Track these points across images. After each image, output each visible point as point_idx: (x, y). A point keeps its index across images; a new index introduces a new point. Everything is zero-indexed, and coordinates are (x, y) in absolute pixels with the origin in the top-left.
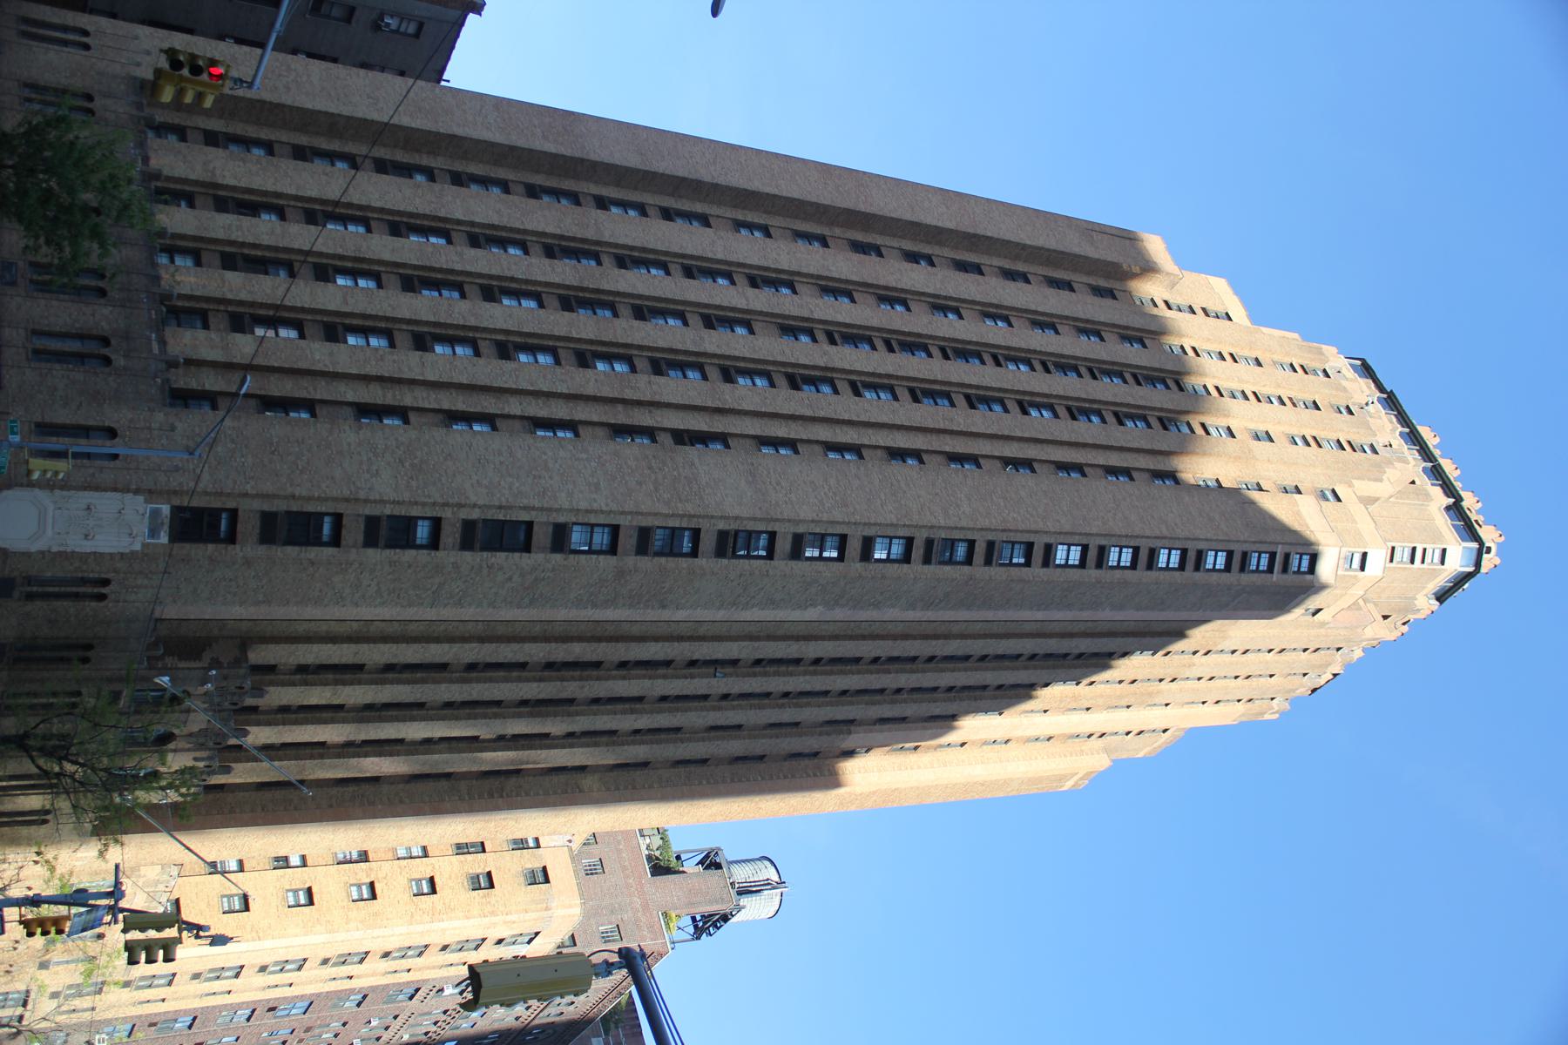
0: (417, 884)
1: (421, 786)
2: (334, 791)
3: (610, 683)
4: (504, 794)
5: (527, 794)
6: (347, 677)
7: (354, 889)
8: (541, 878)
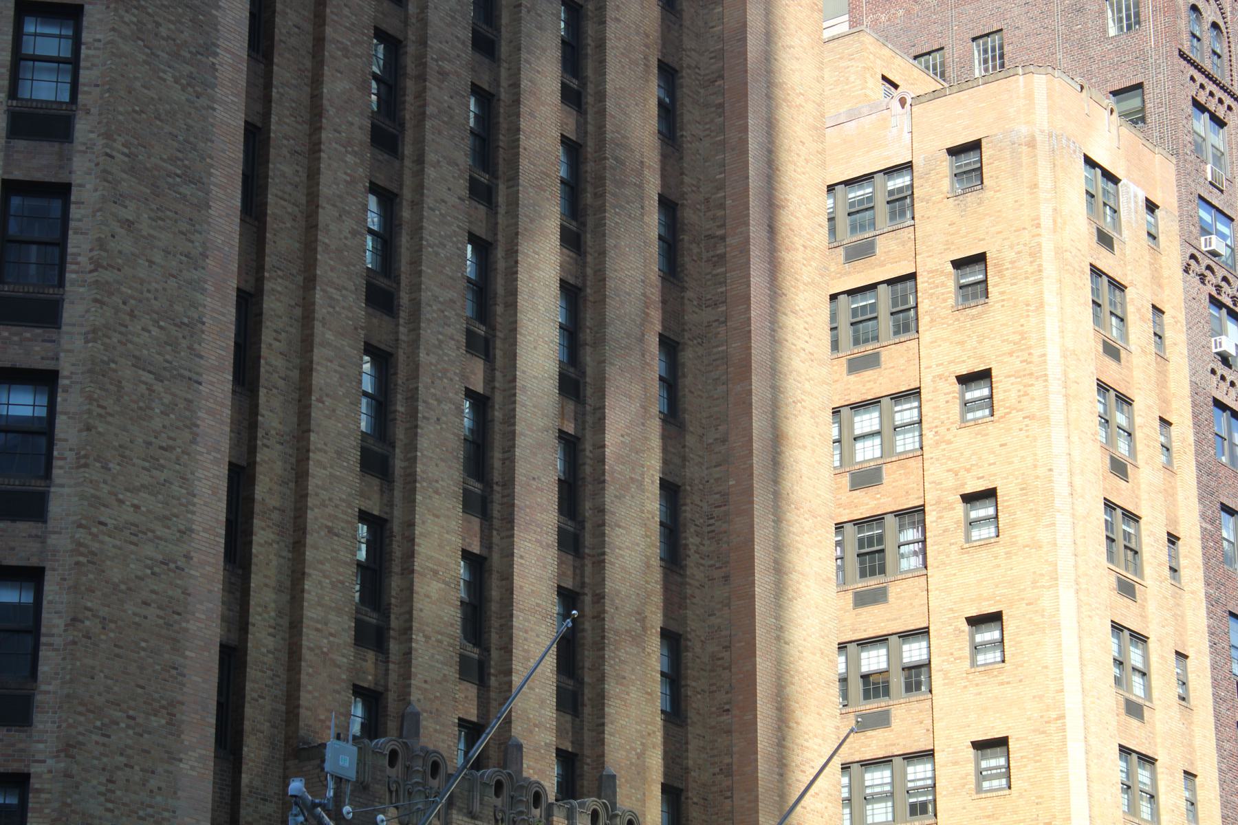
0: (970, 410)
1: (691, 401)
2: (695, 570)
3: (434, 17)
4: (720, 232)
5: (721, 187)
6: (397, 550)
7: (976, 534)
8: (969, 159)
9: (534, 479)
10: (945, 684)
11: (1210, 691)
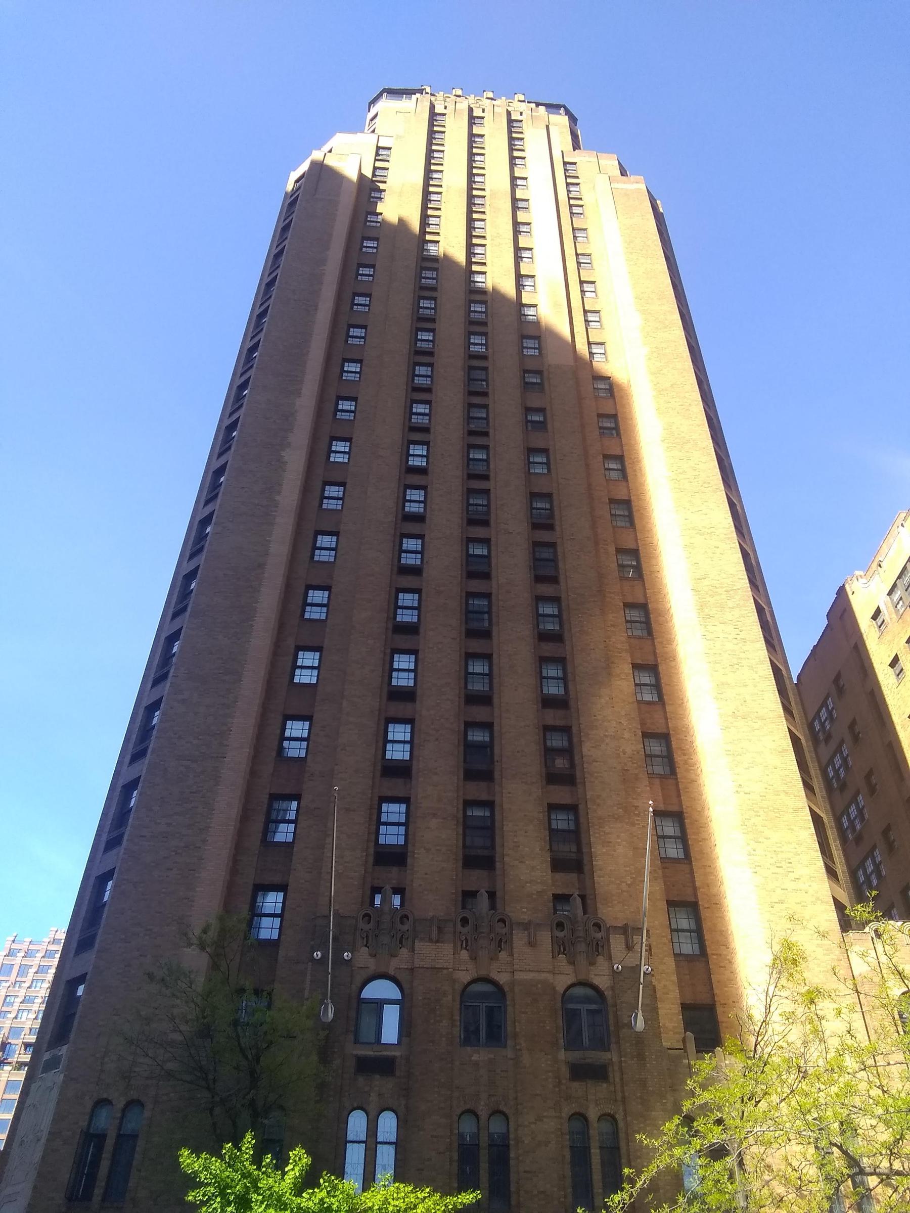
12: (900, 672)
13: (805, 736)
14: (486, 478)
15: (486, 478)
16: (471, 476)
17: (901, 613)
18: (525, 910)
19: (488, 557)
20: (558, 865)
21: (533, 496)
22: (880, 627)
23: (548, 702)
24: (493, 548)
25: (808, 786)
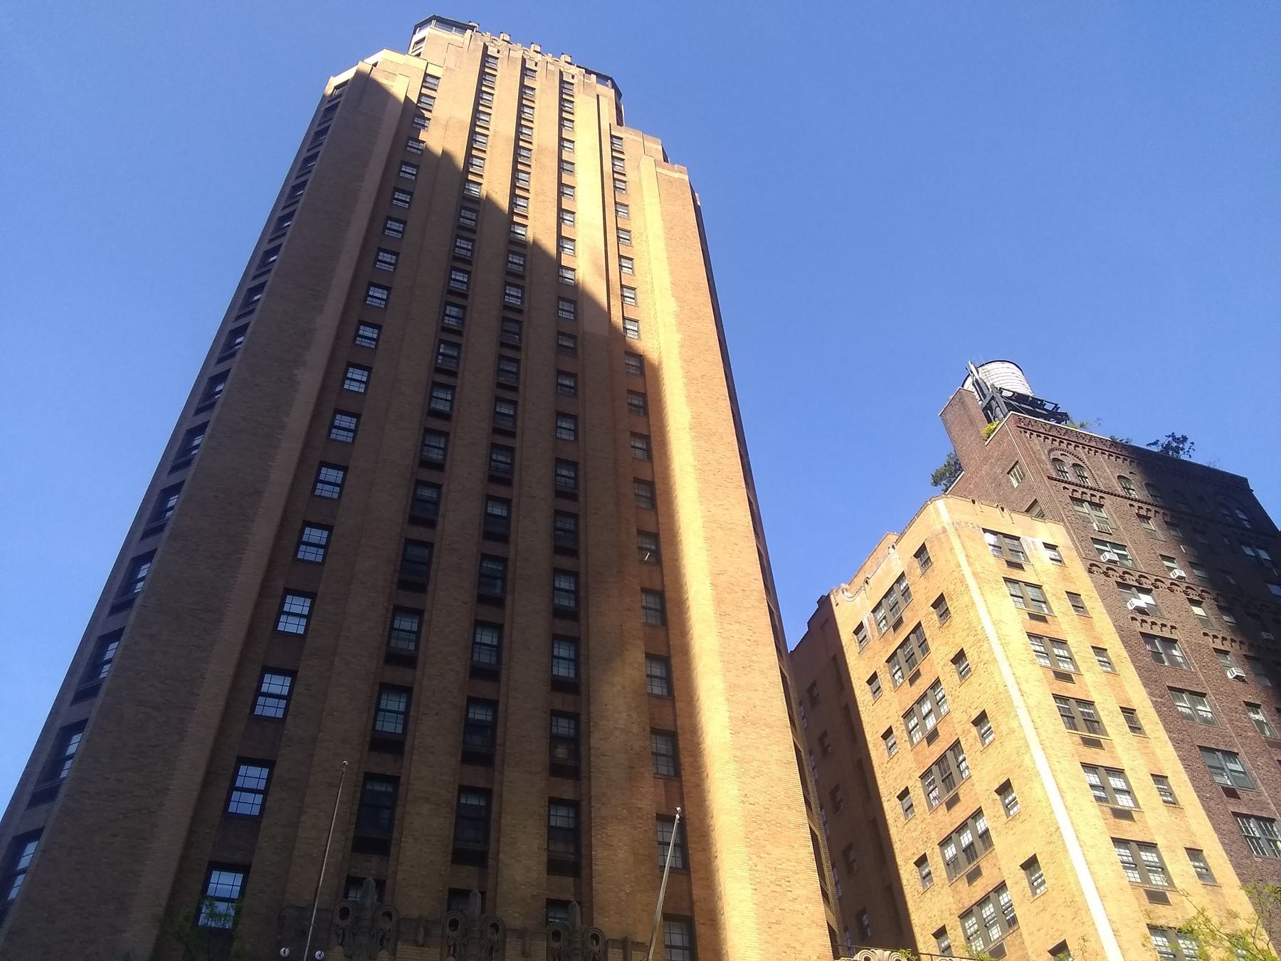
9: (523, 737)
10: (998, 836)
11: (1195, 795)
12: (877, 690)
13: (804, 748)
14: (512, 434)
15: (512, 434)
16: (496, 431)
17: (883, 631)
18: (517, 915)
19: (507, 519)
20: (555, 866)
21: (560, 462)
22: (861, 642)
23: (558, 685)
24: (514, 510)
25: (807, 802)
